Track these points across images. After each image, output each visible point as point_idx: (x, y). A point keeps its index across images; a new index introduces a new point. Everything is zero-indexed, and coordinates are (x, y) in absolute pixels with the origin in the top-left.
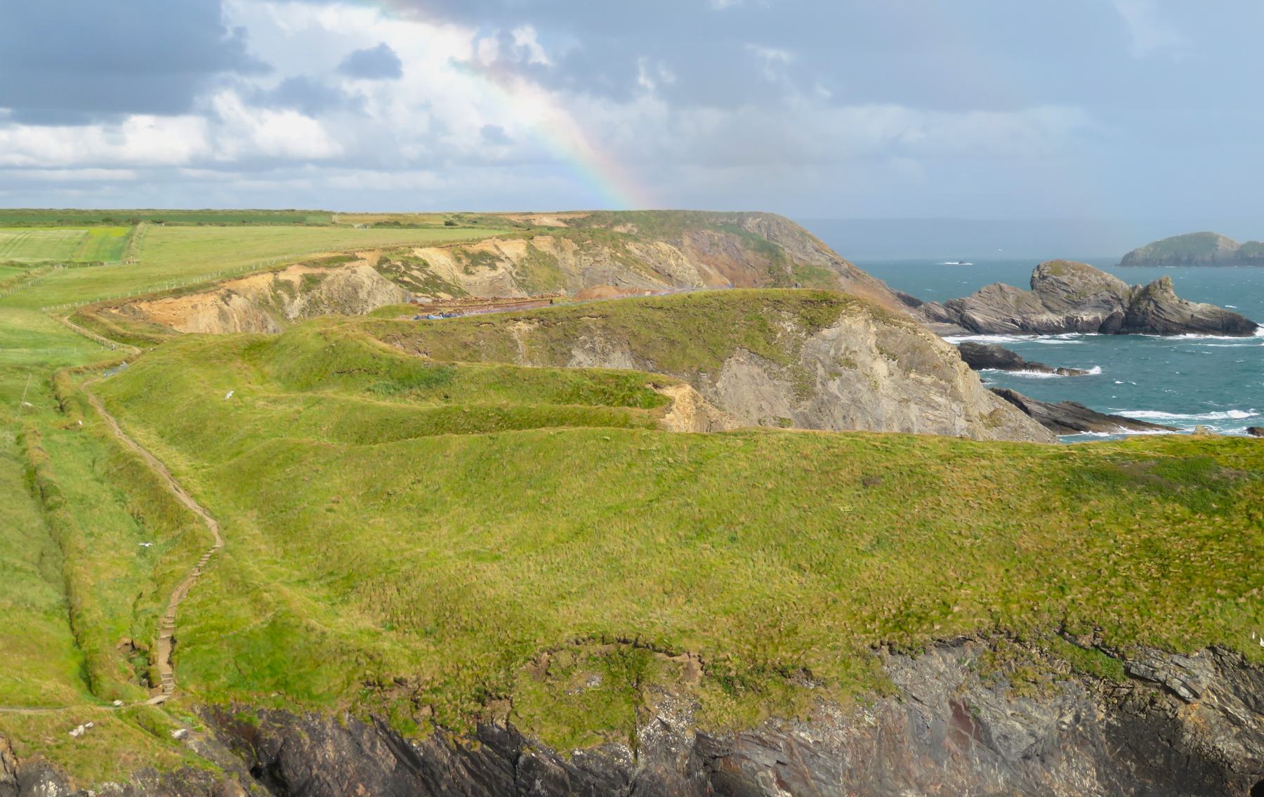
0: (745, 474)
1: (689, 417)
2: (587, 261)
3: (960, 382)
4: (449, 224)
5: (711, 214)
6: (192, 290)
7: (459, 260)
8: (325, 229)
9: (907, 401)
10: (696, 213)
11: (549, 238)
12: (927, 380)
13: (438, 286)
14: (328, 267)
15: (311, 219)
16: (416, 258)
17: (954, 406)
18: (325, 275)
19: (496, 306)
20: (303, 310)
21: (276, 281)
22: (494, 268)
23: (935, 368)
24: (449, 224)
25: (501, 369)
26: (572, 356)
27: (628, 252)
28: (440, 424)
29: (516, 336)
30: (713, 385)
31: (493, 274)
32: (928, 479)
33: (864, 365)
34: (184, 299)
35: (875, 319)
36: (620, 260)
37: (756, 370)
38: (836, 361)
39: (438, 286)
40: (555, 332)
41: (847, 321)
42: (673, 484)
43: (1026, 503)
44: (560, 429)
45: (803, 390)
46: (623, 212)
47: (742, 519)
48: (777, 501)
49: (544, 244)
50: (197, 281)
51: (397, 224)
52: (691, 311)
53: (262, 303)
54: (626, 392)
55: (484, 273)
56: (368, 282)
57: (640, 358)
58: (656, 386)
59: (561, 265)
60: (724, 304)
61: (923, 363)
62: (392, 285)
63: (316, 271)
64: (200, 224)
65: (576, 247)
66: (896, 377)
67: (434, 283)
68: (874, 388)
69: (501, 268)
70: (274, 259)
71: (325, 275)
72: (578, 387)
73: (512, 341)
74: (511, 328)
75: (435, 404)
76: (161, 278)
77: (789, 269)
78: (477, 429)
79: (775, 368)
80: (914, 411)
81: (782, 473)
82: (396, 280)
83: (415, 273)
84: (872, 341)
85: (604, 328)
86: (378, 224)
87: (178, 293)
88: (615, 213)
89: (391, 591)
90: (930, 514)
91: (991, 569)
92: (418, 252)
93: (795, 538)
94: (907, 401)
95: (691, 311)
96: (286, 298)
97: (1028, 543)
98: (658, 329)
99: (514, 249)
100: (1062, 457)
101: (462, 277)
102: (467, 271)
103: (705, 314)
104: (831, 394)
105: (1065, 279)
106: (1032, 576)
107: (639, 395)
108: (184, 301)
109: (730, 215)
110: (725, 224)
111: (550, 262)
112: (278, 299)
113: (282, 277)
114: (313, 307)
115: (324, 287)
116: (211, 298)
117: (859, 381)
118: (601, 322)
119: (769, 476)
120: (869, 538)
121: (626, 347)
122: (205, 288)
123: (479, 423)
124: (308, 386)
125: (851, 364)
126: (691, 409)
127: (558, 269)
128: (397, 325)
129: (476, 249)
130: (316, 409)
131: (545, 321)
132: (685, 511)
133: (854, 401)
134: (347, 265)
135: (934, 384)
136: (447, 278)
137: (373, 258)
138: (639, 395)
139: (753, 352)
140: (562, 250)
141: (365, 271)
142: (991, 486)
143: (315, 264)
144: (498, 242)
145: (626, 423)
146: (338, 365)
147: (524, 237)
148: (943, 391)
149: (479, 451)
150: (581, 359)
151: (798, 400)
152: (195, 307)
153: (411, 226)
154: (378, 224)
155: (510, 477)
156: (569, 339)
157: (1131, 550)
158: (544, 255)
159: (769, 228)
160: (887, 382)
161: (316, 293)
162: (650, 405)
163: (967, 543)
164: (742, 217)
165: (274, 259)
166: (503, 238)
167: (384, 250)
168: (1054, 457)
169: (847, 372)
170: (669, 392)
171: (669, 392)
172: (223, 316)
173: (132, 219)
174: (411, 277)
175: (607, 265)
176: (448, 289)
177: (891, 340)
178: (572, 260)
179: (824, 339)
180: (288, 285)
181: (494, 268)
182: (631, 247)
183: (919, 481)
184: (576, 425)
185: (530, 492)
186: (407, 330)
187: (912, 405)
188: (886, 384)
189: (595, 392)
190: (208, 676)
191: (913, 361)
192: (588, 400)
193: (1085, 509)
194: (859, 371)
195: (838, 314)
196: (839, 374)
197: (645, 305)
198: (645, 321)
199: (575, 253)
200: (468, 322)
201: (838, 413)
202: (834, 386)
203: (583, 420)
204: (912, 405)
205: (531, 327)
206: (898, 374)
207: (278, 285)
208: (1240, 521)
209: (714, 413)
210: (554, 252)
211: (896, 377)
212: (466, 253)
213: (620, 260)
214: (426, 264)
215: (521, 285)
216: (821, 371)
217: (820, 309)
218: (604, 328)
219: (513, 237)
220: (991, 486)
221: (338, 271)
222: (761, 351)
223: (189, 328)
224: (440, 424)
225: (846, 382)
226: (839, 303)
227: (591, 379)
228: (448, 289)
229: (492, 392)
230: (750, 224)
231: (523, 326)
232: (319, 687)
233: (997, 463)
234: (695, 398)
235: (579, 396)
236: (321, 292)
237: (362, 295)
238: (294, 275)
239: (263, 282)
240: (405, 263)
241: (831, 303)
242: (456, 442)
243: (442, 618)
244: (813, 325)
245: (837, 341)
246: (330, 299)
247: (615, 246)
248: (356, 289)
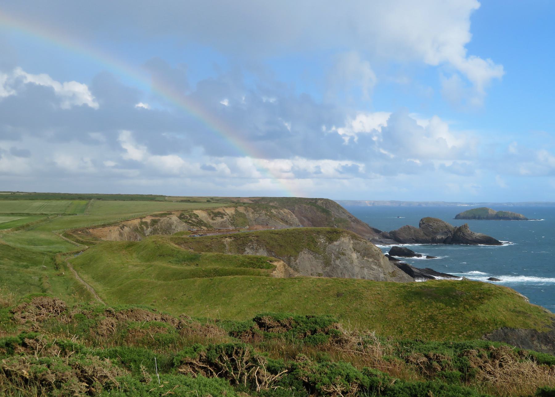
0: (298, 292)
1: (282, 272)
2: (257, 216)
3: (382, 261)
4: (208, 201)
6: (110, 225)
7: (210, 215)
8: (162, 202)
9: (363, 267)
11: (243, 207)
12: (370, 260)
13: (202, 224)
14: (161, 217)
15: (158, 198)
16: (194, 214)
17: (380, 269)
19: (219, 232)
20: (151, 233)
21: (141, 222)
22: (222, 218)
23: (373, 256)
25: (217, 255)
26: (245, 251)
27: (272, 213)
28: (194, 274)
29: (225, 243)
30: (295, 261)
31: (222, 220)
32: (359, 294)
33: (348, 254)
34: (106, 228)
35: (352, 238)
36: (269, 215)
37: (311, 256)
38: (339, 253)
39: (202, 224)
41: (343, 239)
42: (273, 296)
43: (391, 302)
44: (236, 276)
45: (327, 263)
46: (273, 198)
47: (296, 308)
48: (308, 302)
49: (241, 209)
50: (112, 221)
52: (288, 235)
53: (136, 229)
54: (260, 264)
55: (219, 220)
56: (175, 222)
57: (269, 251)
58: (271, 261)
59: (247, 217)
60: (300, 232)
61: (369, 254)
62: (184, 224)
63: (157, 218)
64: (116, 200)
65: (253, 211)
66: (359, 259)
67: (200, 223)
68: (352, 263)
69: (225, 218)
70: (141, 213)
71: (159, 220)
72: (244, 261)
73: (224, 245)
74: (223, 240)
75: (193, 267)
76: (98, 220)
77: (333, 219)
78: (206, 276)
79: (317, 255)
80: (366, 271)
81: (310, 292)
82: (186, 222)
83: (194, 219)
84: (351, 246)
85: (257, 240)
86: (182, 201)
87: (104, 226)
88: (271, 198)
90: (359, 306)
91: (378, 325)
92: (196, 212)
94: (363, 267)
95: (288, 235)
96: (145, 228)
97: (391, 317)
98: (276, 241)
99: (230, 211)
100: (404, 287)
101: (211, 221)
102: (213, 219)
103: (293, 236)
104: (336, 265)
106: (392, 327)
107: (264, 264)
108: (106, 229)
109: (312, 199)
110: (310, 202)
112: (142, 228)
113: (144, 220)
114: (155, 231)
115: (159, 224)
116: (116, 228)
117: (347, 260)
118: (256, 238)
119: (305, 293)
120: (338, 314)
121: (264, 247)
122: (115, 224)
123: (208, 274)
124: (148, 260)
125: (344, 254)
126: (283, 270)
127: (246, 218)
128: (183, 238)
129: (216, 211)
131: (236, 238)
132: (276, 305)
133: (345, 267)
134: (168, 216)
135: (373, 262)
136: (205, 221)
137: (178, 214)
139: (310, 249)
141: (174, 218)
142: (379, 297)
143: (156, 216)
144: (224, 209)
145: (259, 274)
146: (160, 253)
147: (234, 207)
148: (376, 264)
149: (206, 284)
150: (249, 252)
151: (325, 267)
152: (110, 231)
153: (195, 202)
154: (182, 201)
156: (244, 244)
157: (425, 318)
158: (241, 213)
159: (326, 204)
160: (356, 261)
162: (268, 268)
163: (371, 316)
164: (316, 200)
165: (141, 213)
166: (226, 207)
167: (182, 211)
168: (401, 287)
169: (343, 257)
170: (275, 264)
171: (275, 264)
172: (121, 234)
173: (88, 197)
174: (192, 221)
175: (264, 217)
176: (205, 225)
177: (358, 246)
178: (251, 215)
179: (334, 245)
180: (146, 223)
181: (222, 218)
182: (273, 211)
183: (356, 295)
184: (241, 275)
185: (223, 299)
186: (186, 241)
187: (365, 269)
188: (356, 261)
189: (250, 263)
191: (366, 253)
193: (410, 305)
194: (346, 257)
195: (340, 236)
196: (340, 258)
197: (272, 232)
198: (271, 238)
199: (253, 213)
200: (208, 238)
201: (339, 272)
202: (338, 262)
203: (244, 273)
204: (365, 269)
205: (231, 240)
206: (360, 258)
207: (142, 223)
208: (461, 309)
209: (291, 271)
210: (245, 212)
211: (359, 259)
212: (213, 212)
213: (269, 215)
214: (198, 216)
215: (232, 224)
216: (333, 257)
217: (332, 236)
218: (257, 240)
219: (230, 207)
220: (379, 297)
221: (165, 218)
222: (312, 249)
223: (108, 239)
224: (194, 274)
225: (342, 261)
226: (340, 233)
228: (205, 225)
229: (213, 263)
230: (319, 202)
231: (228, 240)
233: (382, 289)
234: (284, 266)
235: (244, 265)
237: (173, 227)
238: (148, 220)
239: (136, 222)
240: (190, 216)
242: (199, 281)
244: (331, 240)
245: (339, 246)
246: (161, 228)
247: (267, 211)
248: (171, 224)
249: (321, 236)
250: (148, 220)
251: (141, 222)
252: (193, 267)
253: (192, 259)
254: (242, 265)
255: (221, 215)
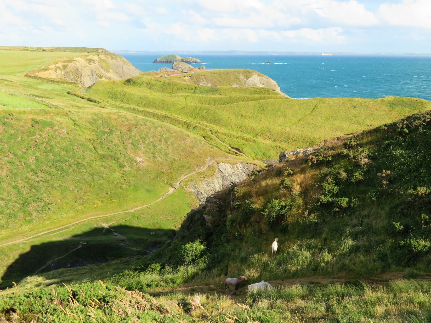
4: (44, 50)
5: (89, 48)
10: (85, 48)
11: (103, 55)
18: (68, 65)
24: (44, 50)
34: (47, 71)
40: (194, 79)
41: (254, 76)
51: (28, 50)
55: (93, 66)
56: (80, 67)
59: (108, 62)
65: (111, 57)
71: (68, 65)
84: (259, 81)
86: (24, 50)
89: (268, 135)
93: (348, 118)
98: (216, 78)
99: (96, 58)
101: (89, 65)
105: (180, 66)
108: (46, 72)
109: (94, 49)
111: (106, 62)
113: (57, 65)
118: (204, 77)
124: (170, 93)
129: (88, 58)
130: (187, 98)
138: (271, 92)
140: (107, 58)
143: (64, 62)
155: (271, 110)
158: (103, 60)
161: (66, 69)
178: (111, 61)
185: (279, 113)
190: (250, 154)
192: (259, 94)
199: (111, 59)
210: (105, 59)
212: (88, 60)
215: (102, 67)
218: (205, 78)
221: (71, 64)
227: (257, 89)
231: (186, 78)
232: (272, 154)
236: (67, 69)
237: (80, 70)
238: (60, 65)
241: (249, 72)
242: (250, 103)
243: (288, 139)
244: (247, 77)
249: (241, 75)
250: (60, 65)
251: (56, 66)
252: (217, 96)
253: (213, 91)
254: (255, 93)
255: (93, 61)
